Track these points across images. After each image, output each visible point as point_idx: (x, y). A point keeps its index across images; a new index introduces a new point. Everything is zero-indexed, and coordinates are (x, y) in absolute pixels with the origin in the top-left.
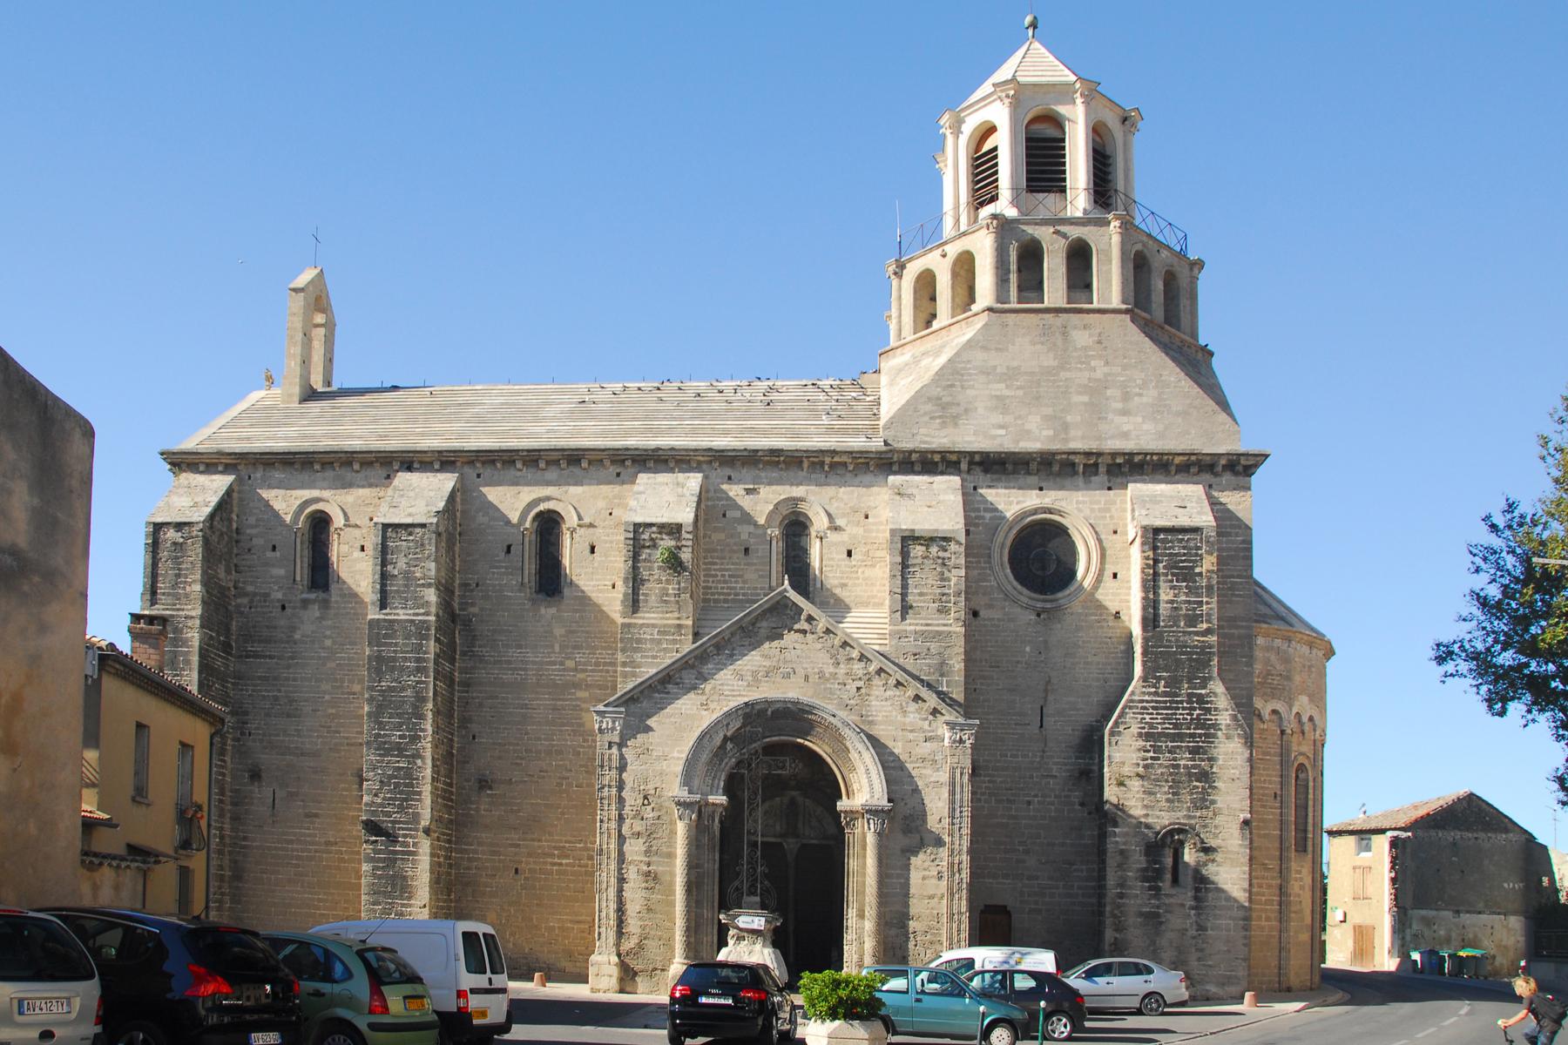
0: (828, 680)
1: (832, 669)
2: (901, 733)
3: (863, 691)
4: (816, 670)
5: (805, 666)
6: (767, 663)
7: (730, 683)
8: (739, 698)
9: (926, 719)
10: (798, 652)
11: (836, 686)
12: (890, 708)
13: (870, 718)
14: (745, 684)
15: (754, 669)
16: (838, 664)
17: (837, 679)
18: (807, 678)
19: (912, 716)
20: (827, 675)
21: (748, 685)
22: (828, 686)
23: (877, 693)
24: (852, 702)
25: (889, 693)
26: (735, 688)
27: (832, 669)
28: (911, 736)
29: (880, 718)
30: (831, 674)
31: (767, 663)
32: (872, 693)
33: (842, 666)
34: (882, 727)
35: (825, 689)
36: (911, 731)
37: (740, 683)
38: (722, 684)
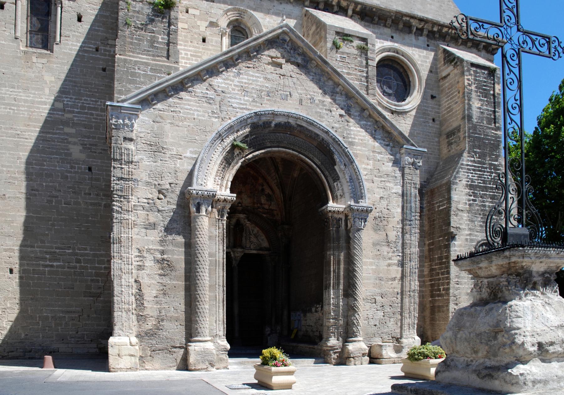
0: (317, 105)
2: (372, 154)
4: (309, 97)
5: (299, 91)
8: (244, 111)
11: (324, 111)
13: (350, 140)
14: (251, 99)
17: (325, 105)
18: (301, 102)
20: (317, 102)
21: (254, 101)
22: (318, 110)
24: (336, 125)
26: (242, 102)
29: (357, 141)
30: (319, 101)
34: (359, 148)
35: (316, 112)
37: (246, 98)
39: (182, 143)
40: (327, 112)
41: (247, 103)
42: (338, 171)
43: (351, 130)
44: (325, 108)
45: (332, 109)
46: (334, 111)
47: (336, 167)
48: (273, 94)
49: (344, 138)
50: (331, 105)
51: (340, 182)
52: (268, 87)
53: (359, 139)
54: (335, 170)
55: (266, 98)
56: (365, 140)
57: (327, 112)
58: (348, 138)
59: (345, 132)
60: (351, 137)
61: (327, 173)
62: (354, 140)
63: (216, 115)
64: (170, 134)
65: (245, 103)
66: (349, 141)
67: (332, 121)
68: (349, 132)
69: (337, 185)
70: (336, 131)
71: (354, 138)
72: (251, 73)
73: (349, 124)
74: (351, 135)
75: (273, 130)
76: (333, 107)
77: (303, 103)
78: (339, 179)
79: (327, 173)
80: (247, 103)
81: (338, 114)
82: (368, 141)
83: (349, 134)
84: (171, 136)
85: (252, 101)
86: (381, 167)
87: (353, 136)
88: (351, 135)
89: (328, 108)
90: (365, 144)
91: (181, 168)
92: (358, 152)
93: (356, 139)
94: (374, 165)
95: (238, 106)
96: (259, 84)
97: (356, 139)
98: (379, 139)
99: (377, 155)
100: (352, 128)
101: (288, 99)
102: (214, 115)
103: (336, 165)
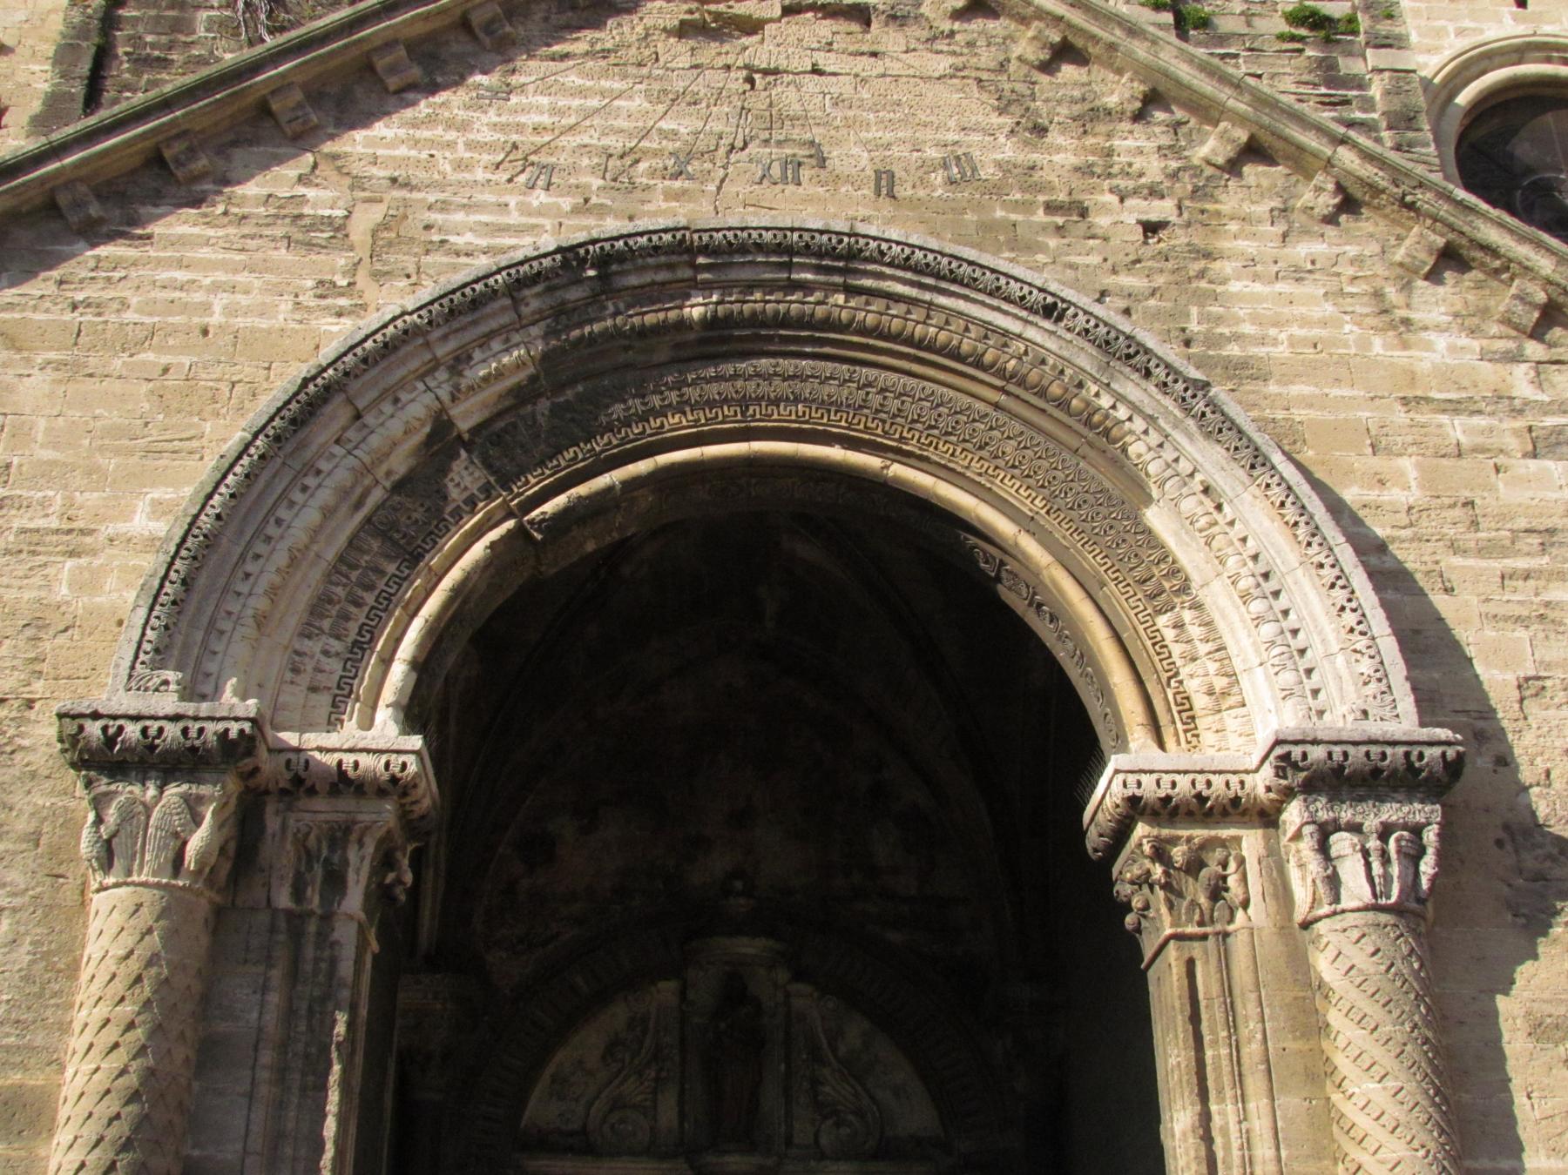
1: (1008, 150)
2: (1400, 416)
3: (1177, 239)
6: (683, 124)
7: (489, 197)
9: (1514, 358)
10: (843, 86)
11: (1040, 216)
12: (1329, 308)
13: (1233, 350)
15: (616, 143)
16: (1041, 131)
19: (1441, 342)
22: (1000, 214)
23: (1248, 246)
24: (1127, 280)
25: (1303, 250)
26: (514, 218)
27: (1008, 150)
28: (1458, 429)
29: (1282, 351)
30: (1004, 167)
31: (683, 124)
32: (1225, 244)
33: (1055, 137)
34: (1297, 389)
36: (1454, 407)
38: (444, 207)
39: (111, 463)
40: (1060, 220)
41: (540, 221)
42: (1171, 542)
43: (1239, 297)
44: (1041, 198)
45: (1088, 200)
46: (1104, 209)
47: (1156, 518)
48: (708, 166)
49: (1187, 343)
50: (1076, 182)
51: (1197, 606)
52: (675, 133)
53: (1293, 342)
54: (1148, 532)
55: (661, 185)
56: (1346, 346)
57: (1060, 220)
58: (1213, 341)
59: (1194, 310)
60: (1237, 337)
61: (1092, 560)
62: (1260, 351)
63: (343, 302)
64: (42, 423)
65: (533, 221)
66: (1228, 359)
67: (1094, 259)
68: (1215, 309)
69: (1179, 626)
70: (1127, 312)
71: (1262, 340)
72: (573, 79)
73: (1217, 265)
74: (1239, 321)
75: (702, 341)
76: (1092, 190)
77: (900, 191)
78: (1184, 589)
79: (1092, 560)
80: (540, 221)
81: (1131, 220)
82: (1365, 344)
83: (1219, 320)
84: (48, 430)
85: (576, 211)
86: (1492, 489)
87: (1248, 329)
88: (1239, 321)
89: (1062, 197)
90: (1343, 361)
91: (81, 604)
92: (1299, 414)
93: (1275, 342)
94: (1428, 479)
95: (483, 242)
96: (621, 123)
97: (1275, 342)
98: (1438, 328)
99: (1444, 419)
100: (1235, 287)
101: (804, 180)
102: (329, 301)
103: (1148, 500)
